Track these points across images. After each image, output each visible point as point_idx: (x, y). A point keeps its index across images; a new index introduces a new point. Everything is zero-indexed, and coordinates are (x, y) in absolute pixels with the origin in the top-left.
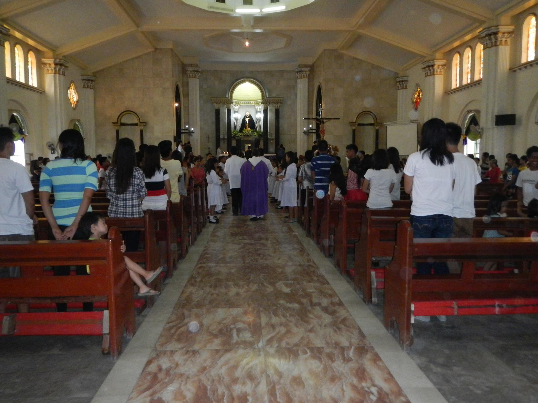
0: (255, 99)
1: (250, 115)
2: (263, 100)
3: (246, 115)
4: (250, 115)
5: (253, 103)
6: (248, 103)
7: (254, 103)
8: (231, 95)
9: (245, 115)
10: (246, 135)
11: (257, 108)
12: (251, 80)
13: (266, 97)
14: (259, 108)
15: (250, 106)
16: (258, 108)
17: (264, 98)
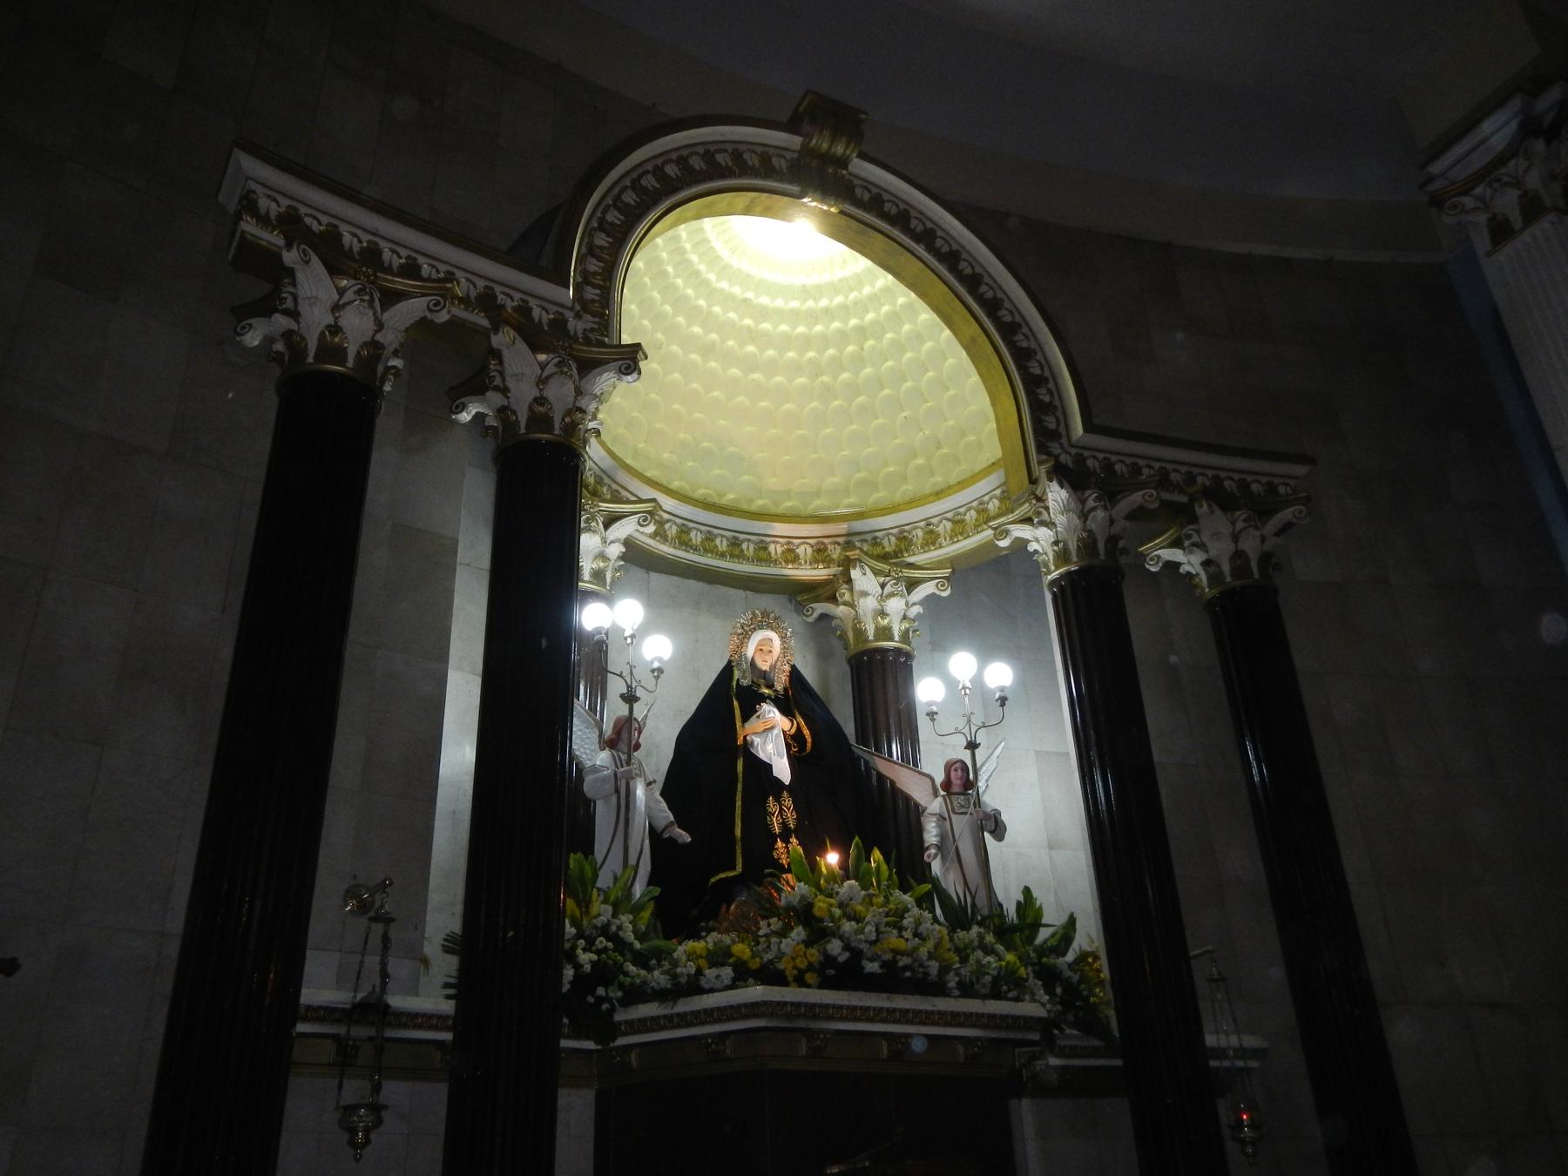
0: (817, 505)
1: (795, 674)
2: (1041, 448)
3: (740, 677)
4: (795, 674)
5: (805, 551)
6: (735, 543)
7: (821, 555)
8: (593, 265)
9: (728, 670)
10: (856, 955)
11: (883, 614)
12: (867, 184)
13: (1089, 426)
14: (905, 617)
15: (740, 594)
16: (895, 605)
17: (1054, 435)
